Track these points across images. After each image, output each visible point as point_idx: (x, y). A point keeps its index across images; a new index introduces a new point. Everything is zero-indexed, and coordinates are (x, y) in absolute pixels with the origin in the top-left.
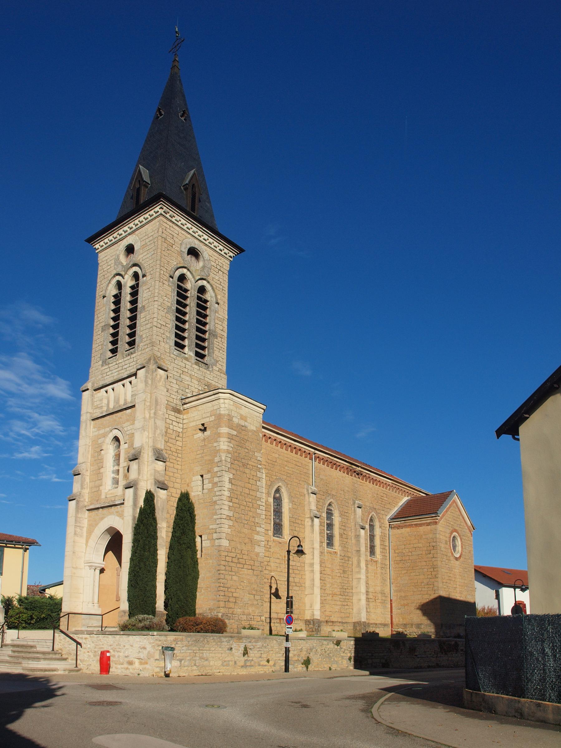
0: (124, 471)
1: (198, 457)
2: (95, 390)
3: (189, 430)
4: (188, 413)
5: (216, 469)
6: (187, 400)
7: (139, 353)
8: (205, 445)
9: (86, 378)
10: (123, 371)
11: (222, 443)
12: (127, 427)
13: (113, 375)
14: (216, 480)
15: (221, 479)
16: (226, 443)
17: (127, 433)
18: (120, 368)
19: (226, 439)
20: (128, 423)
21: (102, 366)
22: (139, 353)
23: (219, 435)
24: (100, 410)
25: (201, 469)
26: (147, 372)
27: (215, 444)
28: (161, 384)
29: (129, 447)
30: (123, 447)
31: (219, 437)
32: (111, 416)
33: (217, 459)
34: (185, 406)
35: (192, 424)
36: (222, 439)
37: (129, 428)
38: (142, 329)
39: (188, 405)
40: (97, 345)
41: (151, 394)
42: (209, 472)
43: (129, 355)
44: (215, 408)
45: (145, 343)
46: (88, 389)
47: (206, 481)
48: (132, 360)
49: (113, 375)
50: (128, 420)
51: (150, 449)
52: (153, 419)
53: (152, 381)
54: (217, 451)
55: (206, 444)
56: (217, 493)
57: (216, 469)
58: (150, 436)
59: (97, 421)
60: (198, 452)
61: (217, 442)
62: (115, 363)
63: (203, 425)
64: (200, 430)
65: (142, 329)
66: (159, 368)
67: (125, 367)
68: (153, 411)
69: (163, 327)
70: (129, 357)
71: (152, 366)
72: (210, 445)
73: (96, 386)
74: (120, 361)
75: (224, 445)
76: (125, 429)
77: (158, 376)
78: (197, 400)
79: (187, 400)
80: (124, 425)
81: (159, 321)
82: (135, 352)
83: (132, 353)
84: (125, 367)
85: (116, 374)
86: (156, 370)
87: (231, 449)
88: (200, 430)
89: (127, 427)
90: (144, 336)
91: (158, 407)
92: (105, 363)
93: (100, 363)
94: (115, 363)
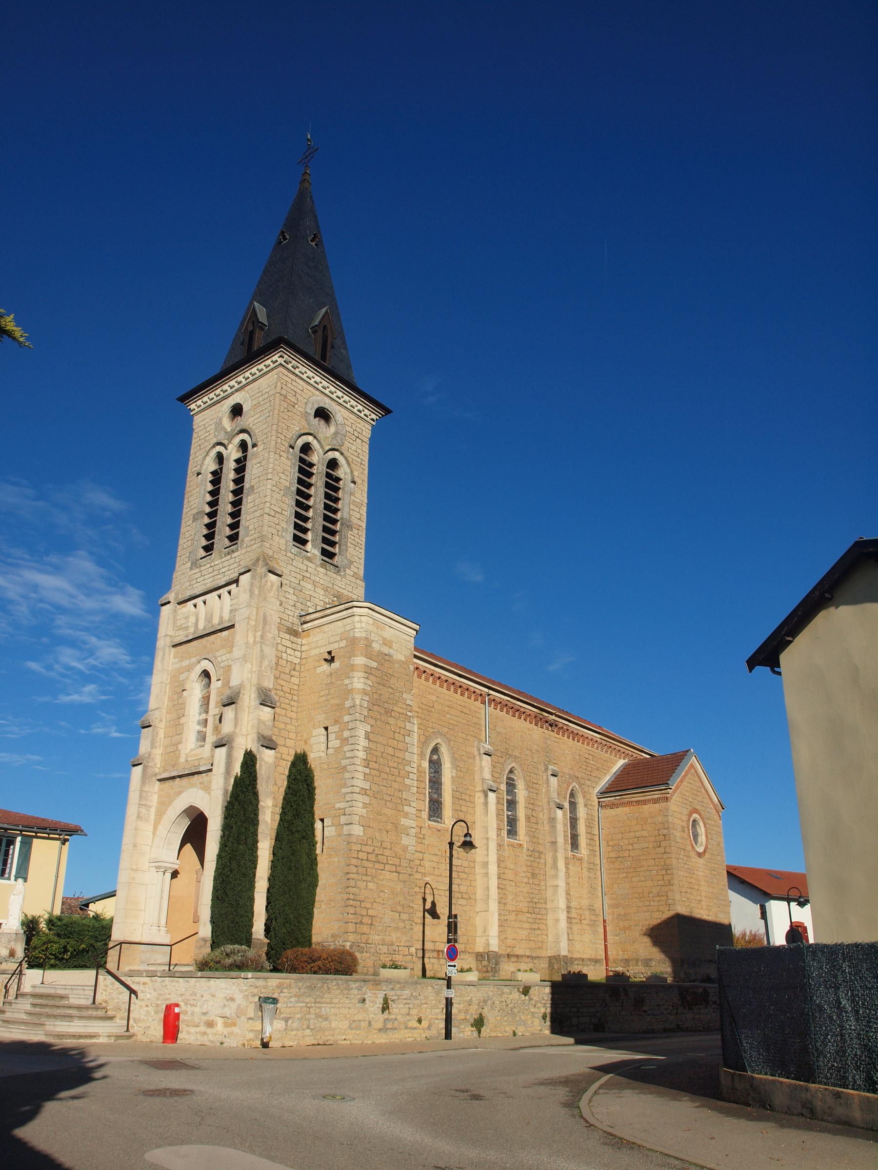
1: (321, 699)
2: (179, 603)
3: (310, 660)
4: (309, 636)
5: (346, 718)
6: (308, 618)
7: (244, 551)
8: (331, 682)
9: (168, 587)
10: (219, 577)
11: (355, 680)
12: (222, 657)
13: (205, 582)
14: (346, 734)
15: (353, 733)
16: (362, 680)
17: (222, 665)
18: (216, 572)
19: (362, 674)
20: (224, 651)
21: (191, 569)
22: (244, 551)
23: (352, 668)
24: (185, 633)
25: (326, 719)
26: (253, 577)
27: (347, 682)
28: (272, 594)
29: (223, 686)
30: (215, 685)
31: (353, 670)
32: (199, 641)
33: (348, 704)
34: (305, 626)
35: (314, 652)
36: (356, 674)
37: (224, 658)
38: (248, 517)
39: (309, 624)
40: (185, 540)
41: (257, 608)
42: (336, 722)
43: (229, 554)
44: (348, 628)
45: (252, 538)
46: (169, 602)
47: (332, 737)
48: (232, 561)
50: (223, 647)
51: (254, 689)
52: (259, 646)
53: (260, 591)
54: (349, 692)
55: (333, 680)
56: (348, 755)
57: (346, 718)
58: (254, 669)
59: (179, 648)
60: (322, 693)
61: (349, 677)
62: (209, 565)
63: (330, 653)
64: (326, 660)
65: (248, 517)
66: (270, 571)
67: (223, 570)
68: (259, 634)
69: (277, 515)
70: (229, 557)
71: (261, 569)
73: (181, 598)
74: (217, 562)
75: (358, 682)
76: (219, 659)
77: (269, 584)
78: (322, 617)
79: (308, 618)
80: (218, 654)
81: (273, 507)
82: (237, 550)
83: (233, 551)
84: (223, 570)
86: (265, 575)
87: (369, 688)
88: (326, 660)
89: (222, 657)
90: (251, 527)
91: (267, 627)
92: (195, 564)
93: (189, 565)
94: (209, 565)
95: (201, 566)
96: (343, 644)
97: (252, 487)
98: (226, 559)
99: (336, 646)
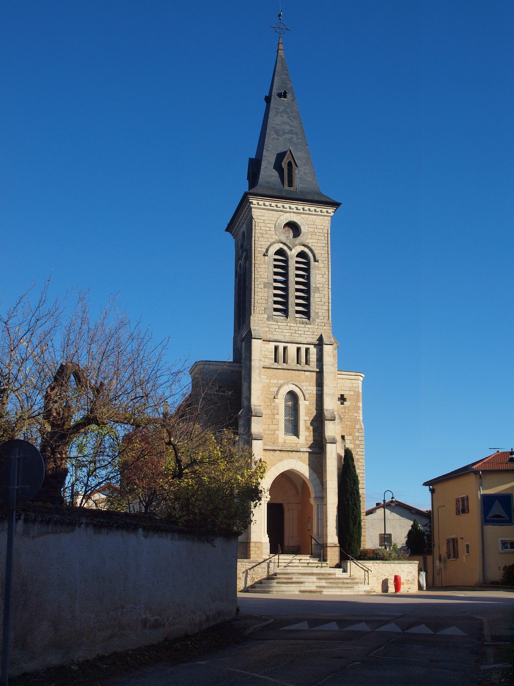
0: (306, 423)
5: (357, 434)
27: (356, 414)
29: (310, 405)
37: (309, 388)
43: (303, 323)
45: (322, 321)
49: (284, 334)
50: (307, 381)
55: (347, 411)
57: (357, 434)
61: (357, 413)
62: (285, 324)
67: (300, 332)
70: (303, 326)
72: (351, 414)
80: (303, 384)
82: (310, 324)
83: (307, 323)
84: (300, 332)
85: (288, 334)
90: (320, 314)
94: (285, 324)
95: (277, 322)
96: (352, 393)
97: (318, 288)
98: (301, 325)
99: (347, 393)
